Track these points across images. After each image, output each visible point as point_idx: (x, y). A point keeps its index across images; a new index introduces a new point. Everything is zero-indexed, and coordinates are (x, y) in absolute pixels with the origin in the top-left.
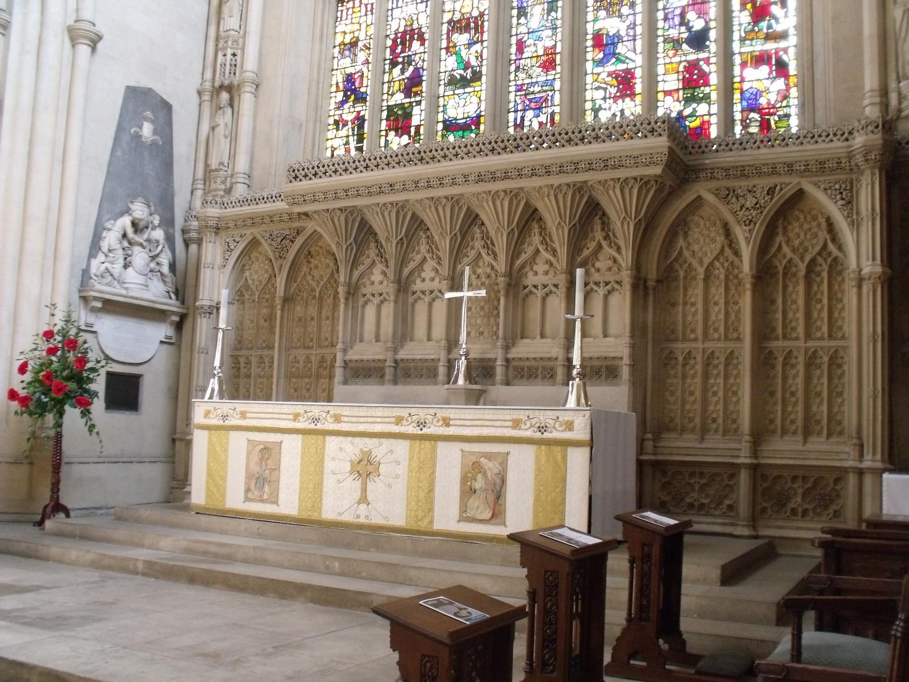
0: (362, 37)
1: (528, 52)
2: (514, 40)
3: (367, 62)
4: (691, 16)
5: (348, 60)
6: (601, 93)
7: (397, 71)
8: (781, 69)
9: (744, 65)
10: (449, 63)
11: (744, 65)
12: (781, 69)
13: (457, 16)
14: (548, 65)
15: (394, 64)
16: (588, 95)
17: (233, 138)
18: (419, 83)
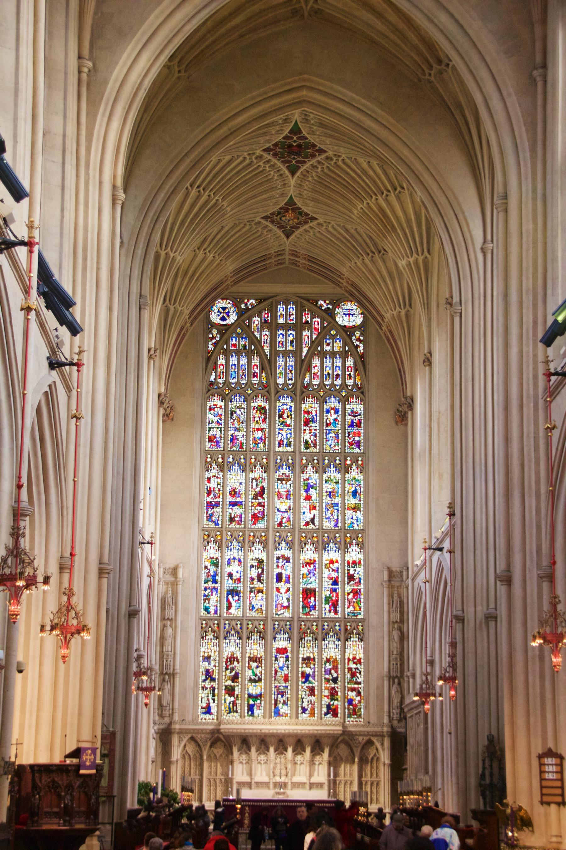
0: (212, 655)
1: (279, 674)
2: (274, 669)
3: (215, 666)
4: (333, 671)
5: (207, 663)
6: (304, 693)
7: (228, 671)
8: (359, 694)
9: (348, 691)
10: (249, 673)
11: (348, 691)
12: (359, 694)
13: (252, 656)
16: (300, 693)
18: (238, 678)
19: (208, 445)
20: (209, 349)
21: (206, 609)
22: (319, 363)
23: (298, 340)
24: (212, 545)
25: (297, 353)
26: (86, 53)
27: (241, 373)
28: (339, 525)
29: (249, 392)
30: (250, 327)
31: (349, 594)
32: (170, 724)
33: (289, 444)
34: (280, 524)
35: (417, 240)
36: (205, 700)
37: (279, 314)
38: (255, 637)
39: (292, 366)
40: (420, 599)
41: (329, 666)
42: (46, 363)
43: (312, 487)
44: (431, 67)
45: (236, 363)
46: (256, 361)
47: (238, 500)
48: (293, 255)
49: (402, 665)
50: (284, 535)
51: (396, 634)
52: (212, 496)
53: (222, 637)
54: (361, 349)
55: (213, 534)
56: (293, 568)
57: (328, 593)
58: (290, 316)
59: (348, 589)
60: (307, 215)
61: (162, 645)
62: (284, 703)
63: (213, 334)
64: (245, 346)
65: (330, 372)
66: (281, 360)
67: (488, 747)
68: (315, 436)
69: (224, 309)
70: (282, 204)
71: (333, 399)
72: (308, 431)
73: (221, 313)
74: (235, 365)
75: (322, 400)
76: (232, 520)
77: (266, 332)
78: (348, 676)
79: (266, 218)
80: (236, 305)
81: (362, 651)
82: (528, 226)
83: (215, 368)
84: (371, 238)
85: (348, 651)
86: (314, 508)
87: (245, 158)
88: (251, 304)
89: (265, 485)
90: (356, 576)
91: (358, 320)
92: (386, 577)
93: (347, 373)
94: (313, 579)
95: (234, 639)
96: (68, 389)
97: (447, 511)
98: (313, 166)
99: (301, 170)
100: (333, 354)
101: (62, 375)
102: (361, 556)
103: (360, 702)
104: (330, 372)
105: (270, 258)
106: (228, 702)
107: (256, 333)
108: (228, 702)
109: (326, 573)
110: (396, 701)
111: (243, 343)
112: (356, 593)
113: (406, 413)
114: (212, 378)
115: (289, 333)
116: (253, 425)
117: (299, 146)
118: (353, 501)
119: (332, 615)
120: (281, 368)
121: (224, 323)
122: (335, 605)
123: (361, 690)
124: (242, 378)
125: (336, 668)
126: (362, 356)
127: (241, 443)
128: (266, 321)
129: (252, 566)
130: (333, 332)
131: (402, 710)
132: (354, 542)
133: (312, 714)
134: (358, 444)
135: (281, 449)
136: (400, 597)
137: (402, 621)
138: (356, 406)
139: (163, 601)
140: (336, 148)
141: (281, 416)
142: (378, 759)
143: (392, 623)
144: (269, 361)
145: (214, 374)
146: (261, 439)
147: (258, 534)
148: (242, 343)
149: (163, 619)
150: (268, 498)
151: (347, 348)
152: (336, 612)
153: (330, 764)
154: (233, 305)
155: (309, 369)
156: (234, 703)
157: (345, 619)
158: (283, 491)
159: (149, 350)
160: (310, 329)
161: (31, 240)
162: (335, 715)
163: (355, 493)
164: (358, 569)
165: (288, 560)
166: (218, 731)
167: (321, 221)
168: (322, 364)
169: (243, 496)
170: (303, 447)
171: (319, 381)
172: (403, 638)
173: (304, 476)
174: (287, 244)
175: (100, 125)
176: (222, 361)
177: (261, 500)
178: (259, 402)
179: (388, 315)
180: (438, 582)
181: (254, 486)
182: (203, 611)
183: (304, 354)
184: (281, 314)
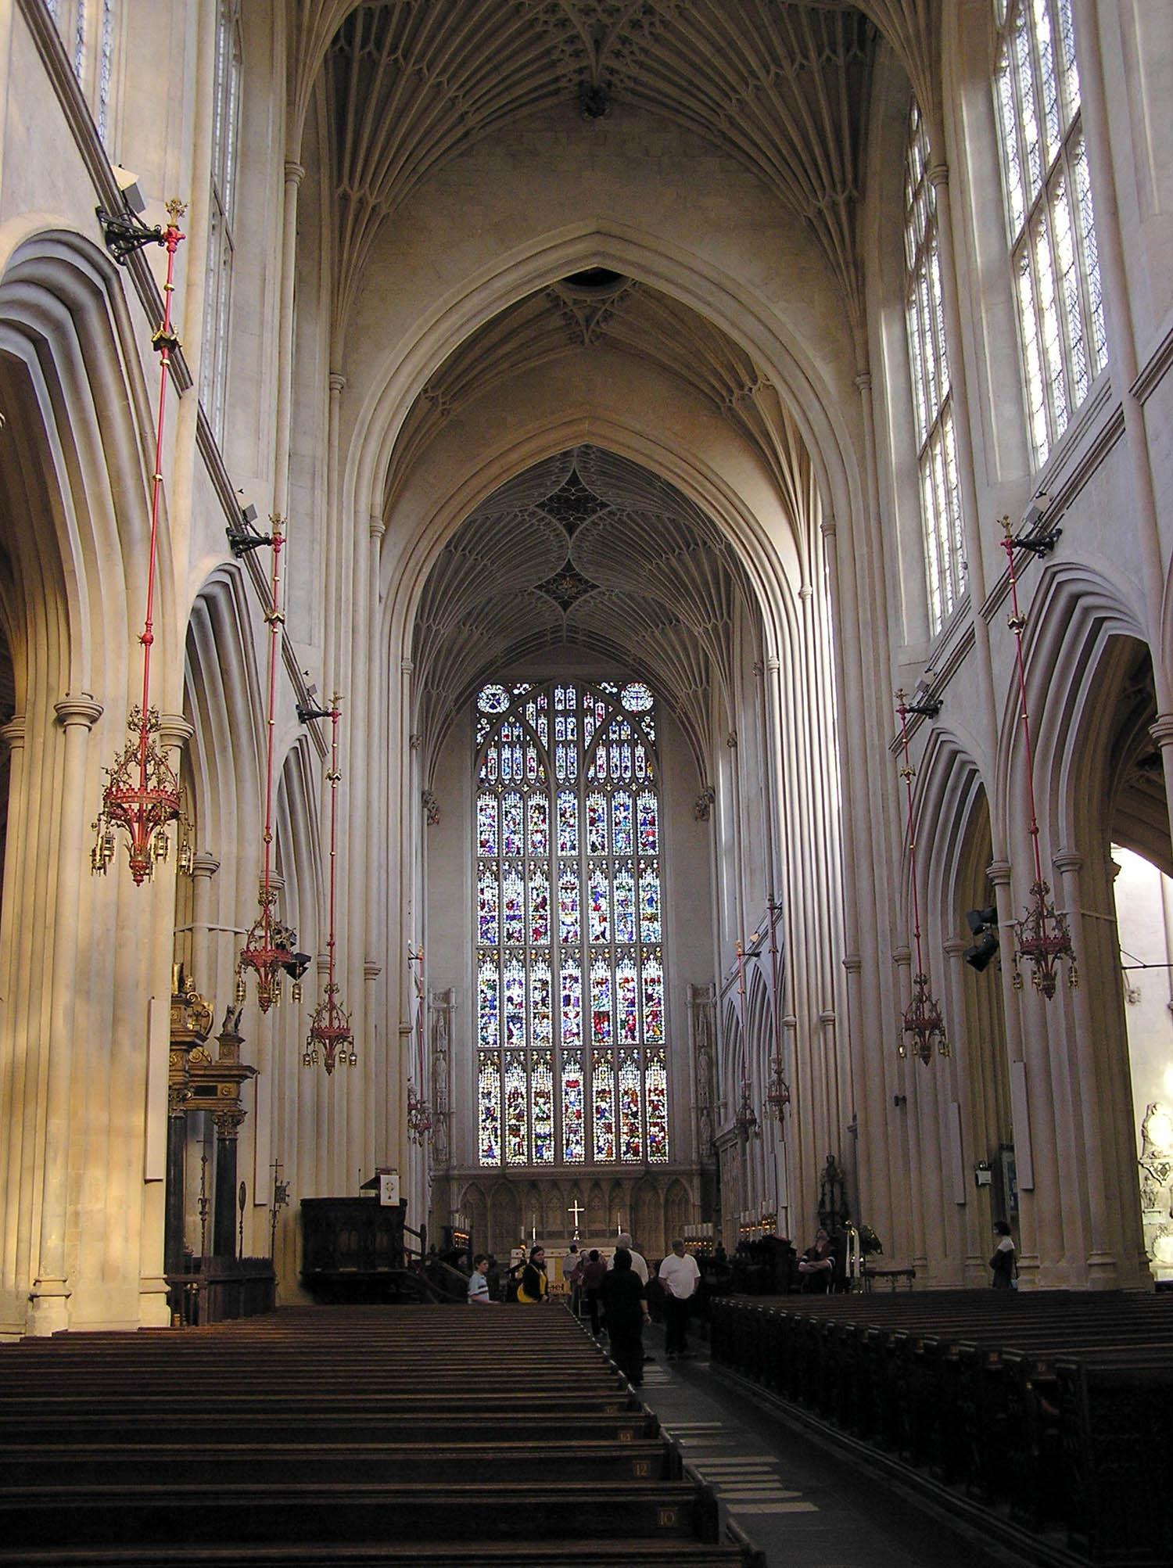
7: (512, 1109)
12: (663, 1129)
14: (578, 1117)
15: (510, 1106)
17: (449, 1137)
19: (480, 851)
21: (484, 1039)
22: (604, 754)
23: (580, 726)
24: (488, 965)
25: (579, 743)
26: (338, 367)
27: (515, 768)
28: (634, 938)
29: (526, 789)
31: (647, 1017)
32: (448, 1170)
33: (573, 848)
34: (566, 940)
36: (486, 1142)
38: (541, 1068)
40: (730, 1019)
41: (627, 1099)
42: (295, 712)
43: (601, 896)
44: (731, 392)
46: (532, 753)
47: (517, 912)
48: (571, 631)
49: (711, 1091)
50: (570, 951)
51: (703, 1059)
52: (486, 909)
53: (503, 1070)
54: (652, 737)
55: (488, 952)
56: (583, 989)
57: (623, 1017)
59: (646, 1011)
60: (587, 582)
61: (435, 1081)
62: (577, 1143)
64: (518, 737)
67: (827, 1169)
68: (603, 837)
69: (494, 695)
70: (559, 570)
71: (622, 794)
72: (594, 832)
75: (609, 795)
76: (510, 936)
77: (543, 720)
78: (649, 1109)
79: (540, 587)
80: (508, 691)
81: (664, 1081)
82: (862, 550)
84: (661, 606)
85: (648, 1081)
86: (605, 919)
87: (516, 516)
88: (525, 689)
89: (548, 896)
90: (655, 995)
91: (649, 704)
92: (689, 992)
94: (605, 1001)
95: (518, 1071)
96: (322, 753)
97: (767, 904)
98: (594, 523)
99: (580, 528)
100: (620, 743)
101: (314, 730)
102: (661, 973)
103: (664, 1138)
105: (545, 635)
106: (512, 1143)
108: (512, 1143)
109: (620, 993)
110: (705, 1136)
112: (655, 1015)
113: (707, 806)
114: (483, 774)
115: (569, 720)
116: (530, 828)
117: (578, 499)
118: (649, 911)
119: (630, 1041)
121: (495, 711)
122: (632, 1030)
123: (665, 1125)
125: (635, 1103)
127: (518, 848)
129: (536, 988)
130: (619, 718)
131: (713, 1144)
132: (652, 957)
133: (610, 1154)
134: (653, 845)
135: (564, 853)
136: (705, 1016)
137: (710, 1045)
138: (648, 800)
139: (435, 1030)
140: (619, 500)
141: (562, 815)
142: (687, 1201)
143: (698, 1048)
144: (548, 752)
145: (484, 770)
146: (541, 842)
147: (541, 952)
149: (435, 1051)
150: (551, 909)
152: (633, 1038)
153: (631, 1208)
154: (504, 691)
155: (594, 761)
156: (520, 1145)
157: (643, 1047)
158: (568, 901)
159: (411, 738)
160: (593, 715)
161: (278, 536)
162: (636, 1153)
163: (651, 901)
164: (657, 988)
165: (576, 980)
166: (504, 1176)
167: (603, 589)
169: (522, 908)
170: (589, 850)
172: (712, 1064)
173: (591, 883)
174: (565, 618)
175: (355, 446)
176: (493, 753)
177: (543, 912)
178: (537, 800)
179: (683, 694)
180: (754, 993)
181: (535, 897)
182: (480, 1042)
183: (586, 744)
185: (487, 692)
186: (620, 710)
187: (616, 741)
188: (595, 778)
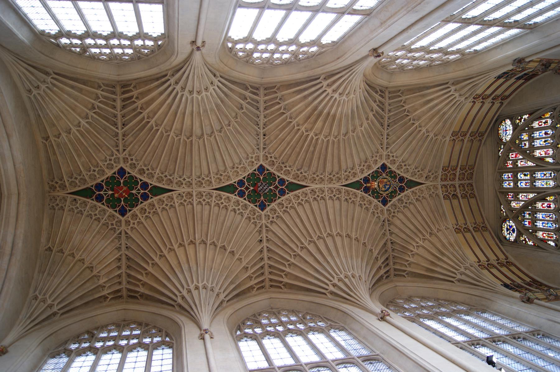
20: (532, 244)
22: (538, 151)
25: (532, 171)
27: (548, 218)
30: (515, 209)
35: (313, 89)
37: (508, 186)
39: (541, 174)
45: (541, 222)
46: (539, 205)
58: (509, 178)
63: (523, 240)
64: (529, 214)
65: (543, 140)
66: (537, 184)
69: (507, 230)
73: (510, 232)
74: (543, 223)
77: (521, 196)
83: (544, 241)
93: (543, 126)
100: (532, 139)
104: (543, 140)
107: (521, 205)
111: (527, 215)
114: (552, 244)
115: (519, 178)
120: (543, 184)
124: (551, 218)
126: (530, 114)
128: (512, 197)
144: (538, 193)
145: (550, 242)
148: (527, 216)
151: (527, 129)
155: (542, 159)
168: (539, 148)
171: (550, 149)
176: (540, 234)
183: (533, 165)
184: (508, 184)
185: (506, 234)
186: (513, 140)
187: (530, 144)
188: (553, 157)
